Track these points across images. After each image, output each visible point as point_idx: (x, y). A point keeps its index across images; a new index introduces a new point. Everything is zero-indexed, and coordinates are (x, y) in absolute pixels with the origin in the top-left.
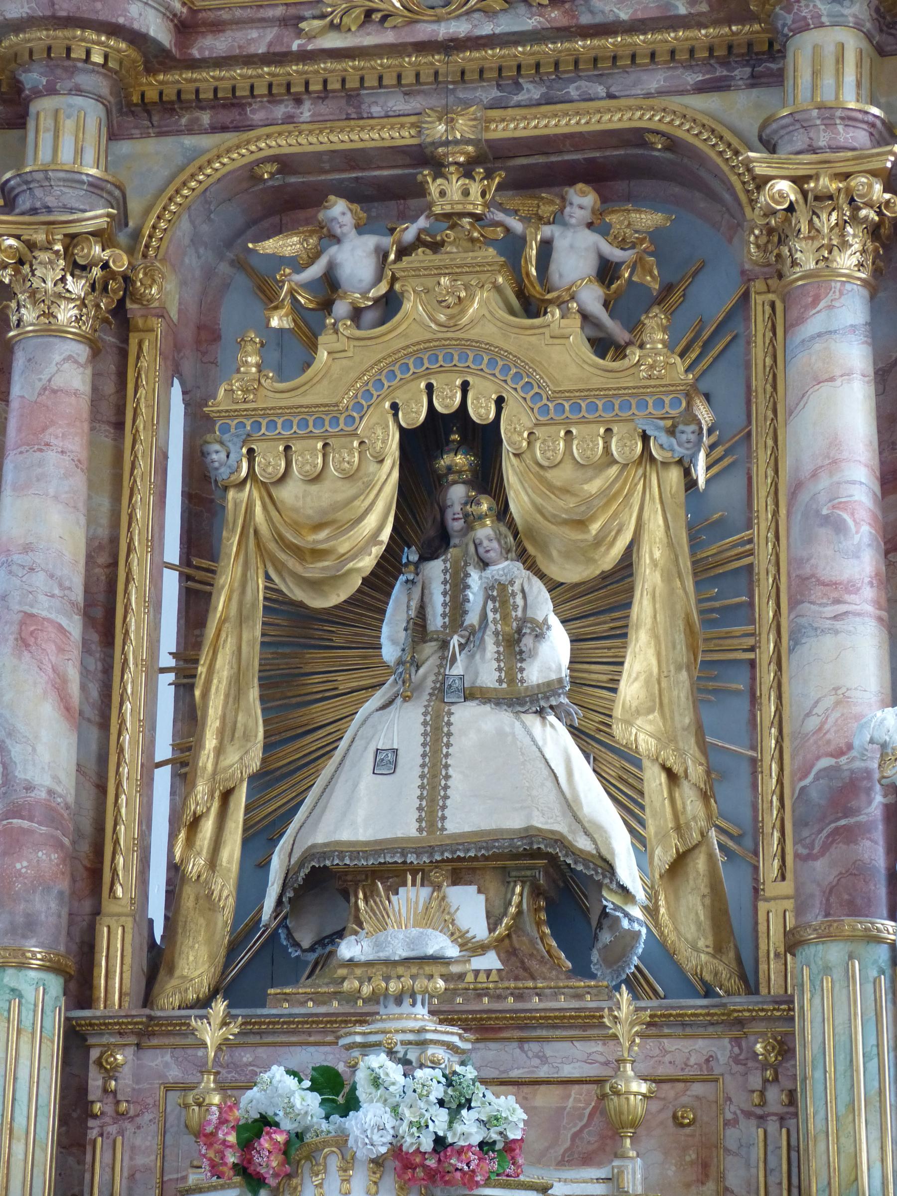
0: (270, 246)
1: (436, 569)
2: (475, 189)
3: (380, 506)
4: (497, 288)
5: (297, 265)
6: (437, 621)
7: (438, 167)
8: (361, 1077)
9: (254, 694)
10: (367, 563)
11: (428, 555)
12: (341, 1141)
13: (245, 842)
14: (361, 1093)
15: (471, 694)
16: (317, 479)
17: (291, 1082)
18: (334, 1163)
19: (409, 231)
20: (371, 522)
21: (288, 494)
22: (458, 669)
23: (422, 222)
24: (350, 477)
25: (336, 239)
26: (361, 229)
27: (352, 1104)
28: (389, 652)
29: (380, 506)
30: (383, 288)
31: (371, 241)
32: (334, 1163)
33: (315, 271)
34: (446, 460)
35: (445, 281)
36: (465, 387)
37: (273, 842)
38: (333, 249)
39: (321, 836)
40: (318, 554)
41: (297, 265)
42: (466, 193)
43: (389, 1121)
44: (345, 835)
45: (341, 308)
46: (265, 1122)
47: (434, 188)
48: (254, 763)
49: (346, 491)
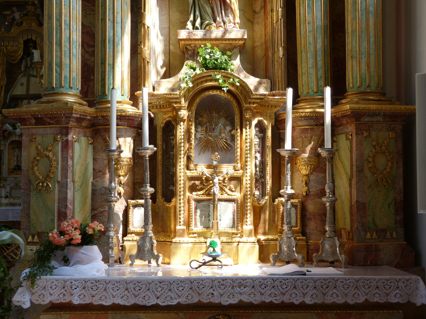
0: (5, 13)
1: (29, 58)
2: (33, 8)
3: (21, 50)
4: (35, 22)
5: (9, 15)
6: (29, 65)
7: (28, 5)
8: (17, 126)
9: (5, 74)
10: (19, 58)
11: (28, 56)
12: (15, 133)
13: (4, 92)
14: (17, 127)
15: (33, 76)
16: (12, 46)
17: (9, 126)
18: (14, 135)
19: (24, 12)
20: (20, 52)
21: (9, 48)
22: (31, 73)
23: (26, 11)
24: (17, 46)
25: (15, 13)
26: (18, 11)
27: (16, 129)
28: (23, 69)
29: (21, 50)
30: (20, 20)
31: (19, 13)
32: (14, 135)
33: (11, 17)
34: (30, 44)
35: (29, 21)
36: (32, 35)
37: (9, 92)
38: (14, 14)
39: (14, 94)
40: (13, 56)
41: (9, 15)
42: (32, 8)
43: (20, 131)
44: (17, 94)
45: (15, 22)
46: (6, 130)
47: (27, 7)
48: (5, 82)
49: (16, 48)
